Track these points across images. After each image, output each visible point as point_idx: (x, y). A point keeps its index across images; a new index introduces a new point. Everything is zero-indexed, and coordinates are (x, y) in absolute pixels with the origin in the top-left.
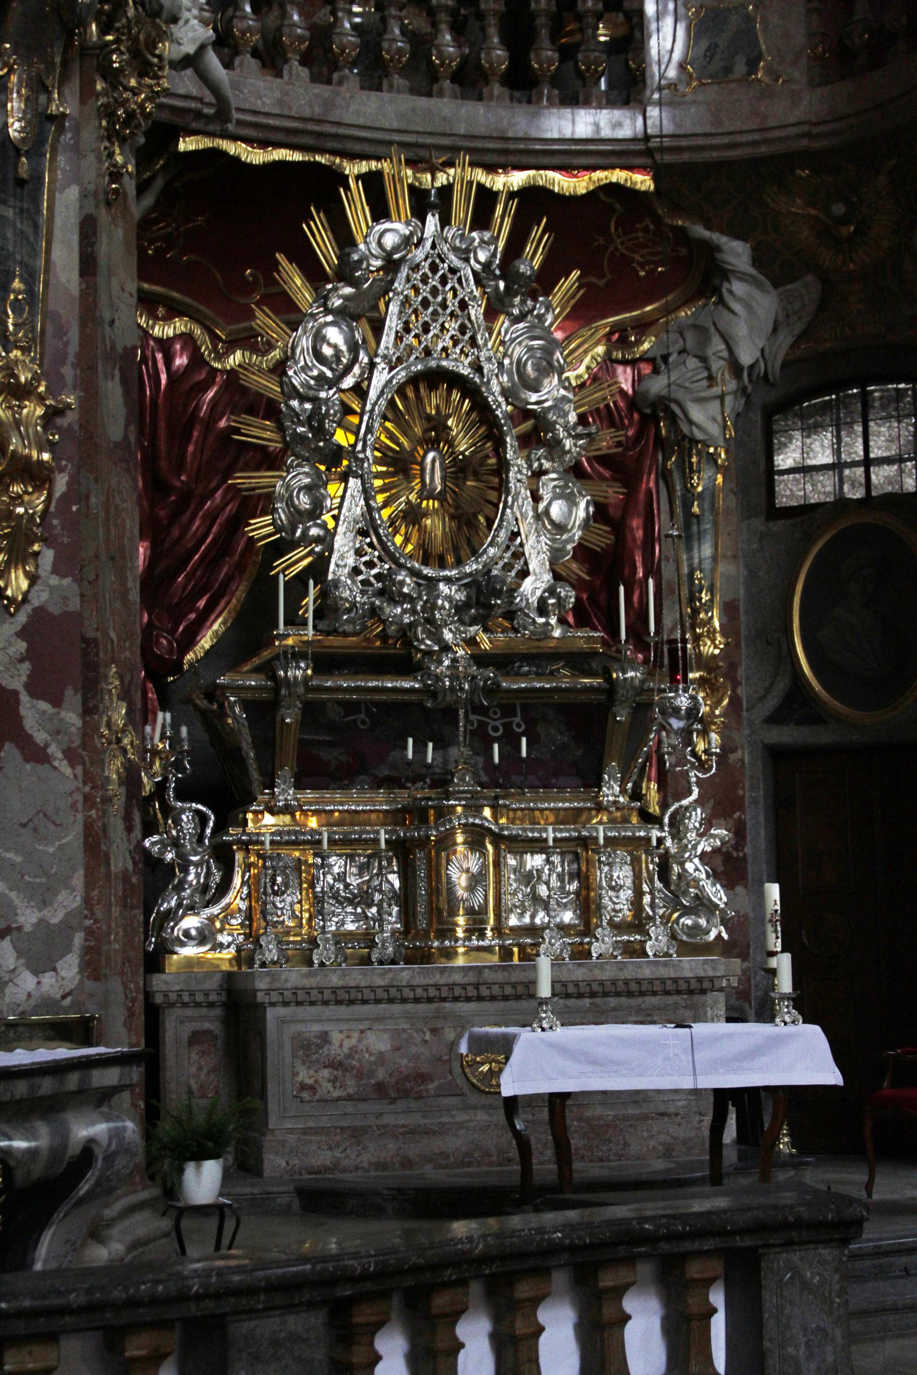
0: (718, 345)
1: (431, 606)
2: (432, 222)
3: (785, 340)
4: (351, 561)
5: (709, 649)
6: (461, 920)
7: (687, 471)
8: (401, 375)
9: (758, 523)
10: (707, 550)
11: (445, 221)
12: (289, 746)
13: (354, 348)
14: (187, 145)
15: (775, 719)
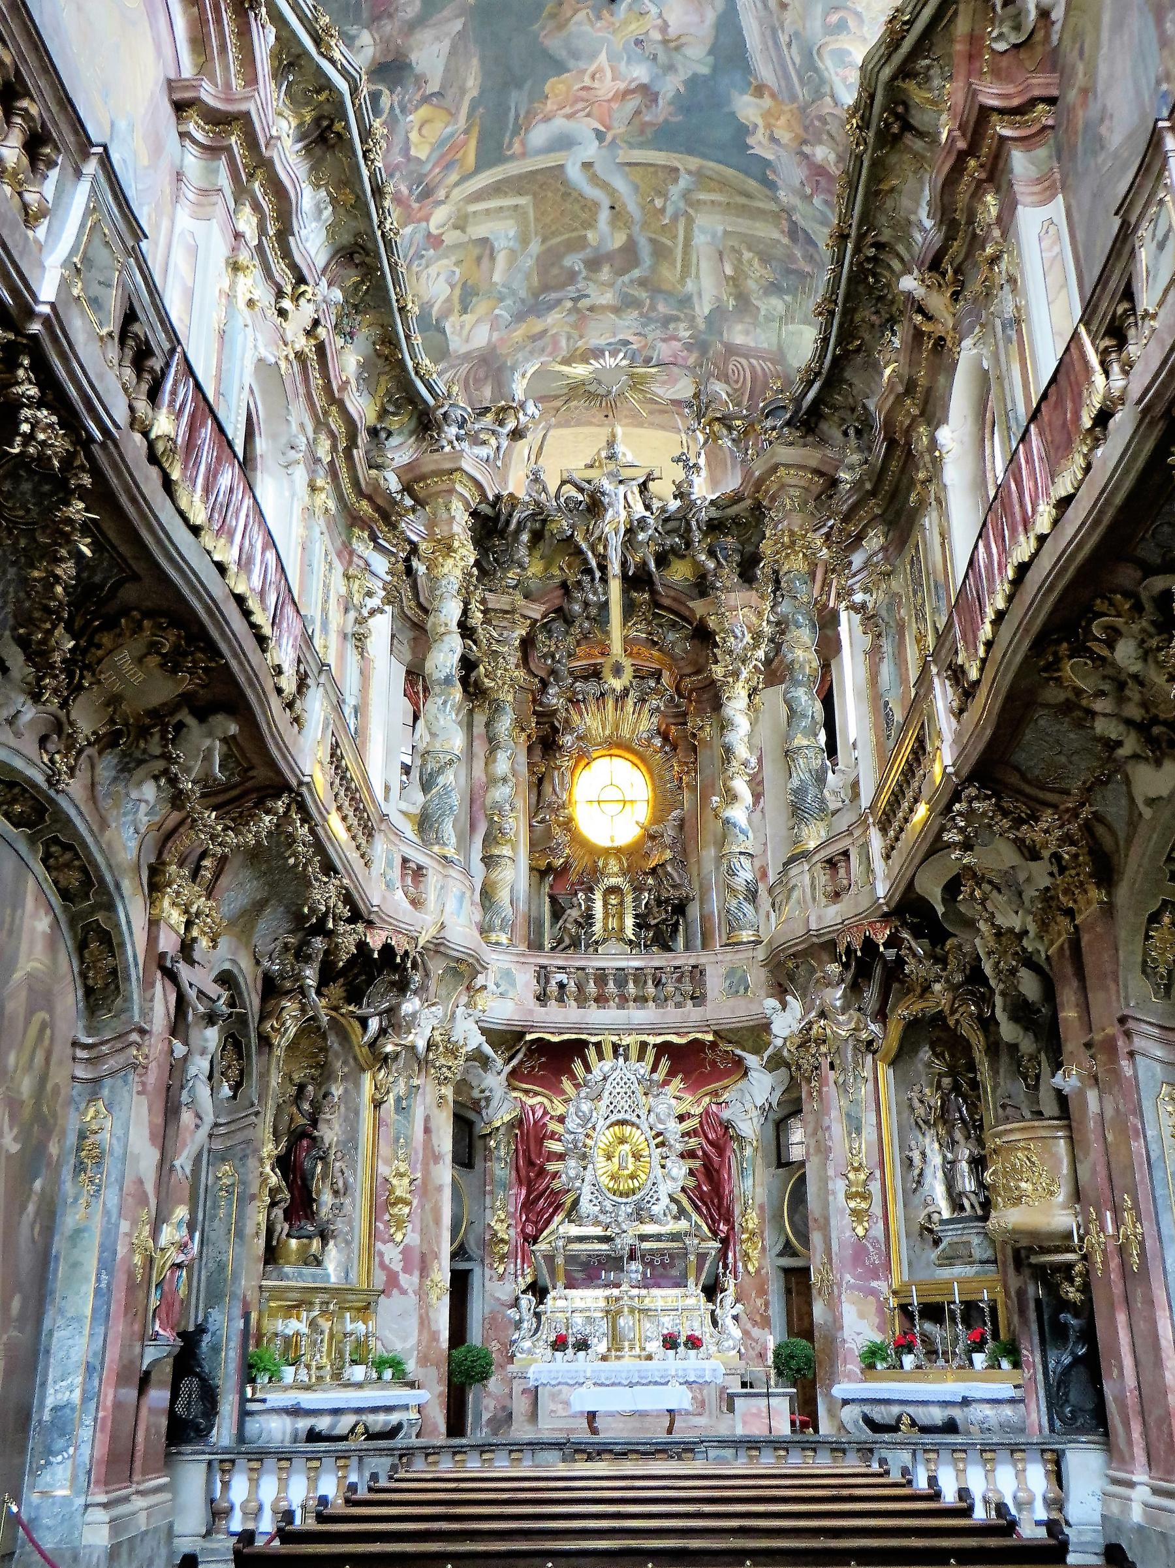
0: (748, 1097)
1: (617, 1215)
2: (621, 1059)
3: (777, 1094)
4: (590, 1197)
5: (751, 1226)
6: (626, 1344)
7: (742, 1149)
8: (608, 1122)
9: (772, 1170)
10: (750, 1182)
11: (626, 1059)
12: (561, 1272)
13: (591, 1111)
14: (529, 1037)
15: (780, 1255)
